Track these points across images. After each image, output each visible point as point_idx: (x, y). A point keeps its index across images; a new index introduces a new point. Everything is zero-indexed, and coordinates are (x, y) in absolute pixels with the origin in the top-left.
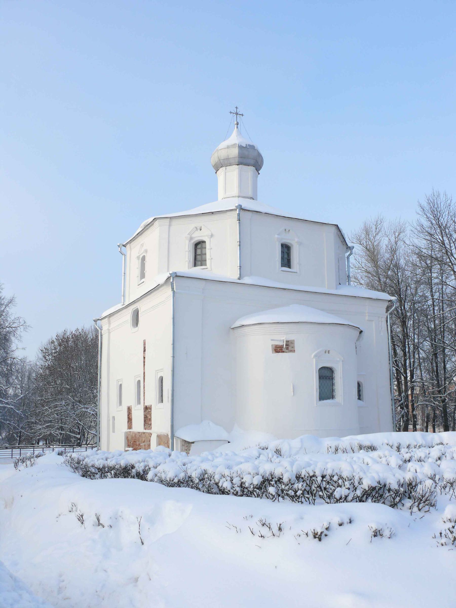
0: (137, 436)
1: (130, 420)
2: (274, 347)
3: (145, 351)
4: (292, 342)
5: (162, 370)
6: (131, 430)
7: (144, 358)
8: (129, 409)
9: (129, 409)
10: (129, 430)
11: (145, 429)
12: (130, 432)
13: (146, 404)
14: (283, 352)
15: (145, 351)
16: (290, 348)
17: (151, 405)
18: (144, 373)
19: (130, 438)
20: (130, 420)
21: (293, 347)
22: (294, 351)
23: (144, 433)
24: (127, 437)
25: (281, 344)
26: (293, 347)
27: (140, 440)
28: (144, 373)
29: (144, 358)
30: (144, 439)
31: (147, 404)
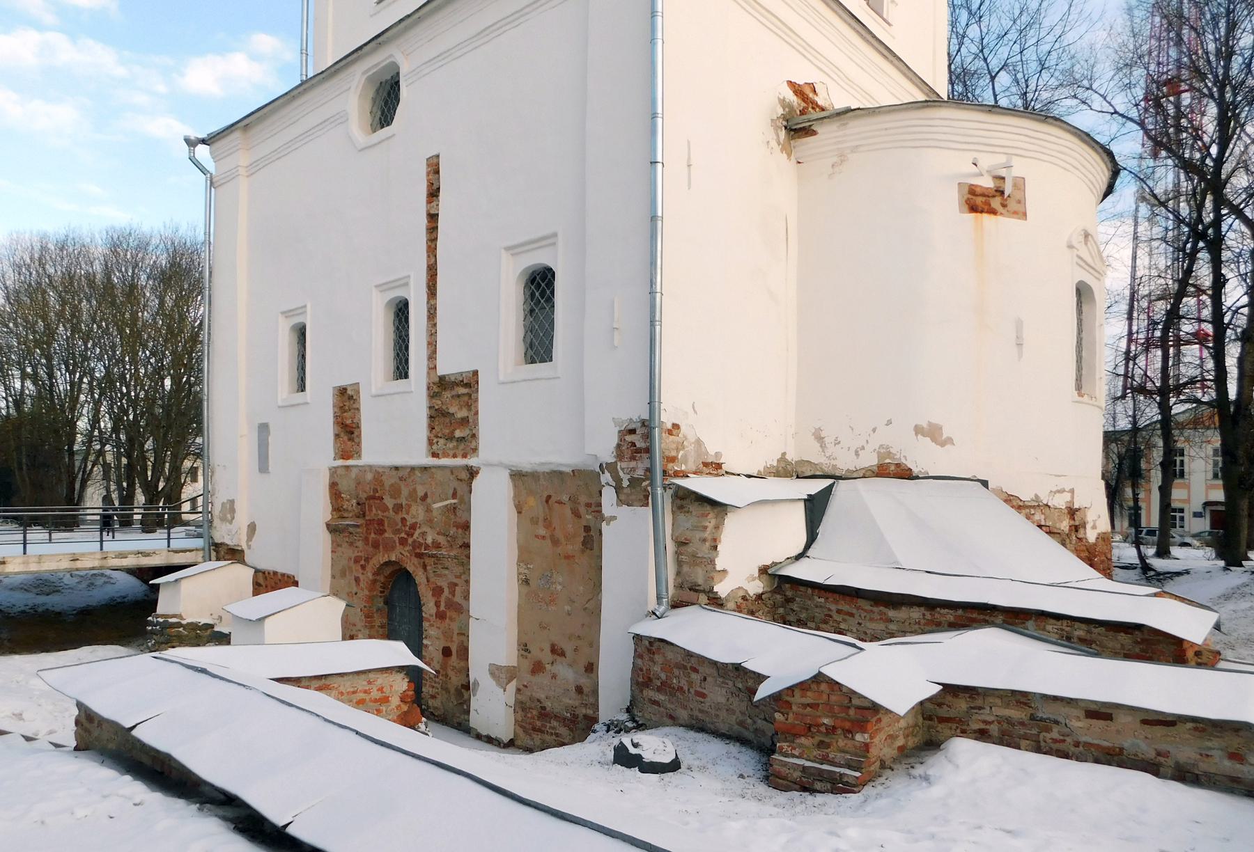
0: (388, 483)
1: (348, 431)
2: (966, 189)
3: (433, 194)
4: (1020, 184)
5: (549, 240)
6: (350, 462)
7: (433, 218)
8: (346, 399)
9: (346, 399)
10: (340, 462)
11: (435, 455)
12: (347, 467)
13: (442, 370)
14: (993, 212)
15: (433, 194)
16: (1012, 205)
17: (476, 373)
18: (432, 271)
19: (346, 485)
20: (348, 431)
21: (1019, 202)
22: (1025, 214)
23: (425, 469)
24: (333, 485)
25: (987, 183)
26: (1019, 202)
27: (405, 492)
28: (432, 271)
29: (433, 218)
30: (420, 493)
31: (446, 367)
